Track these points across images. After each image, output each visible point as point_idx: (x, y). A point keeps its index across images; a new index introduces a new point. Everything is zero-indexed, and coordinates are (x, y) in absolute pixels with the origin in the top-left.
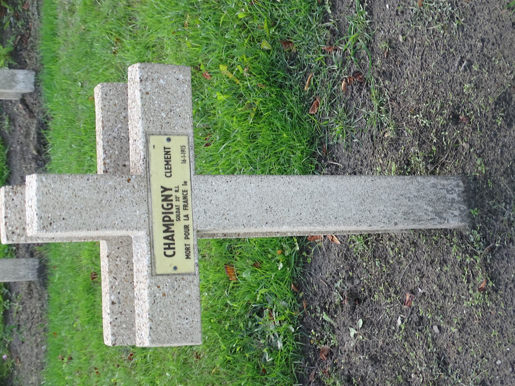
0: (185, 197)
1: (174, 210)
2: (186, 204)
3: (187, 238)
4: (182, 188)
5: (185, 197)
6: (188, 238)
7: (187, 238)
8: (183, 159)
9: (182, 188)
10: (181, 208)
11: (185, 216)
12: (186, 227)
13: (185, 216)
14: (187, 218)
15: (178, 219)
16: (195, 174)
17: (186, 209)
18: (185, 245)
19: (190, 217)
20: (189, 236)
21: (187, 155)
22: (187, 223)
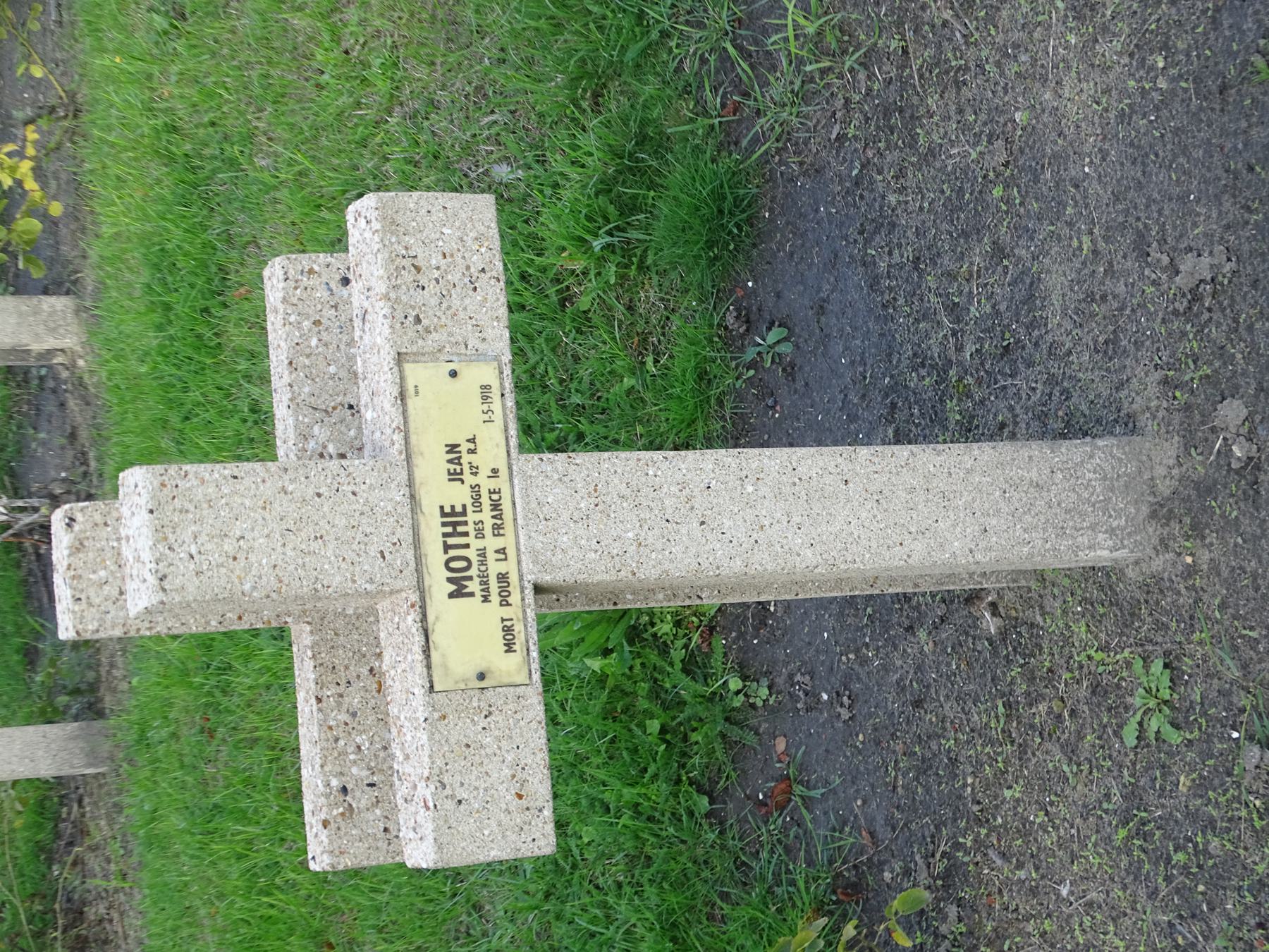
0: (496, 506)
2: (499, 522)
3: (505, 603)
5: (496, 506)
7: (505, 603)
8: (486, 417)
10: (488, 531)
11: (497, 551)
12: (502, 577)
13: (497, 551)
14: (503, 556)
16: (520, 453)
17: (499, 535)
18: (503, 620)
19: (511, 552)
20: (510, 600)
21: (497, 406)
22: (502, 567)
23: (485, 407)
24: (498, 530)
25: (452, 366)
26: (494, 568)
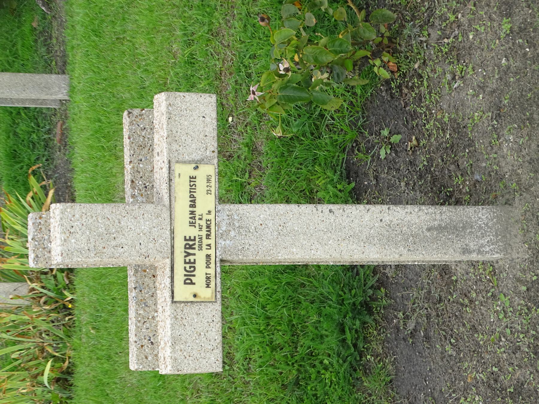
0: (208, 227)
1: (197, 240)
2: (209, 233)
4: (205, 217)
5: (208, 227)
6: (209, 268)
7: (208, 267)
8: (208, 189)
9: (205, 217)
10: (204, 237)
11: (207, 245)
12: (208, 256)
13: (207, 245)
14: (209, 248)
15: (200, 248)
18: (206, 274)
21: (213, 184)
22: (209, 252)
23: (208, 184)
24: (208, 236)
25: (194, 165)
26: (205, 252)
